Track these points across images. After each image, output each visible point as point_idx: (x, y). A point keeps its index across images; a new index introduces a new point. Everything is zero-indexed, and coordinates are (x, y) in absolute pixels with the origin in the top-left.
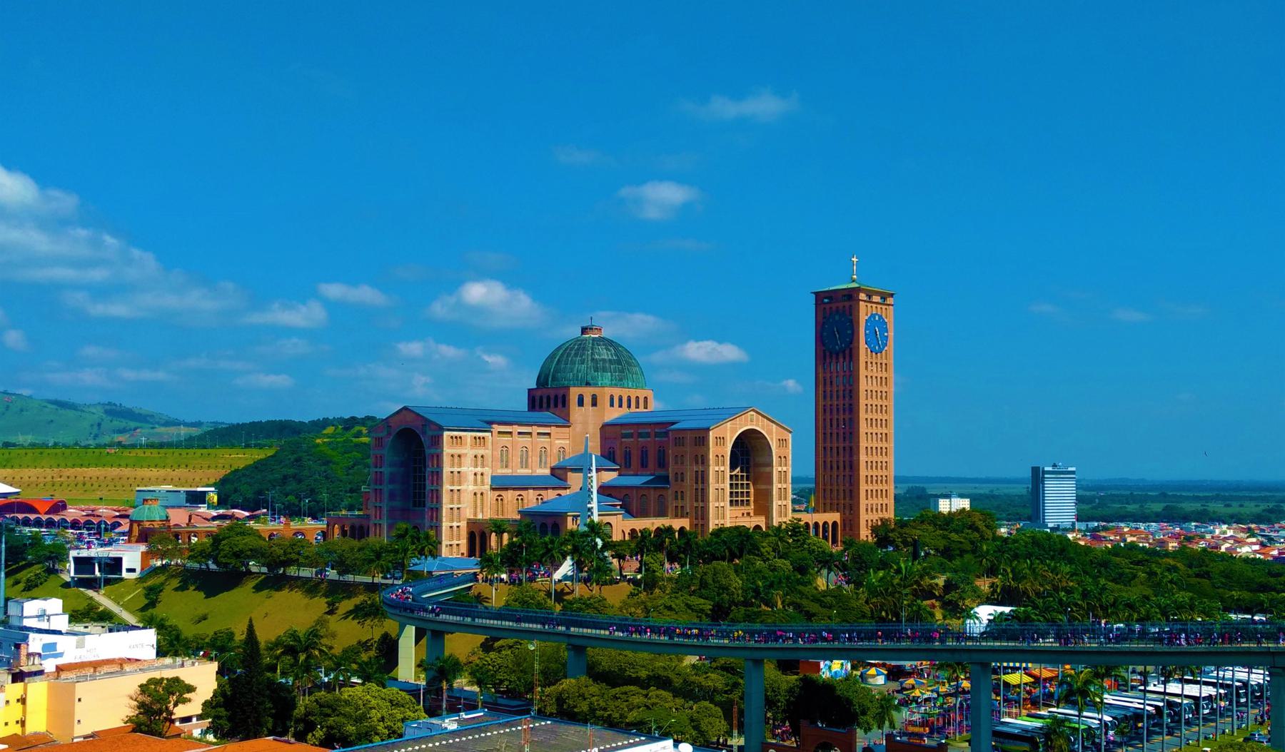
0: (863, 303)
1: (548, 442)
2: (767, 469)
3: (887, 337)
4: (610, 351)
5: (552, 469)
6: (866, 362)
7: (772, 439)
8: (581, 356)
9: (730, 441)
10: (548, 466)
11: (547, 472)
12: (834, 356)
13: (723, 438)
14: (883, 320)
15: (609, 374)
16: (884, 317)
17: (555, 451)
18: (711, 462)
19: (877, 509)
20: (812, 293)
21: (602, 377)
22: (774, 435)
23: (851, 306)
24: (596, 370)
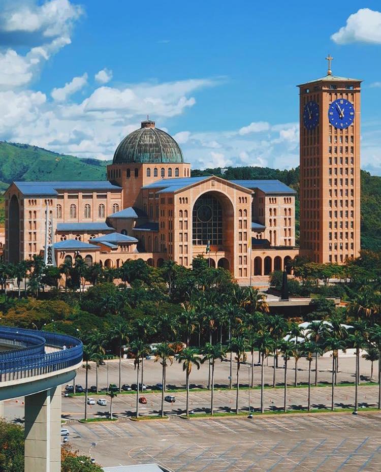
0: (326, 93)
1: (104, 201)
2: (231, 219)
3: (353, 115)
4: (152, 138)
5: (108, 219)
6: (331, 137)
7: (233, 198)
8: (132, 143)
9: (193, 200)
10: (106, 216)
11: (104, 220)
12: (310, 131)
13: (187, 198)
14: (349, 103)
15: (148, 154)
16: (350, 100)
17: (110, 206)
18: (176, 215)
19: (341, 248)
20: (297, 86)
21: (143, 156)
22: (235, 194)
23: (318, 95)
24: (140, 152)
